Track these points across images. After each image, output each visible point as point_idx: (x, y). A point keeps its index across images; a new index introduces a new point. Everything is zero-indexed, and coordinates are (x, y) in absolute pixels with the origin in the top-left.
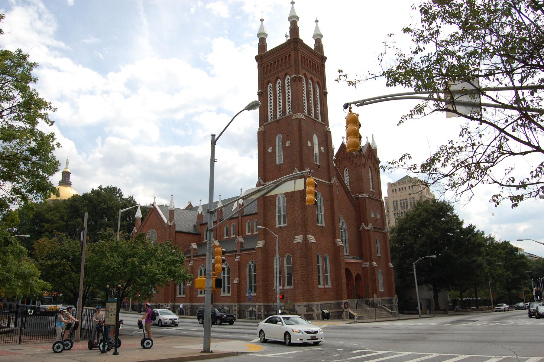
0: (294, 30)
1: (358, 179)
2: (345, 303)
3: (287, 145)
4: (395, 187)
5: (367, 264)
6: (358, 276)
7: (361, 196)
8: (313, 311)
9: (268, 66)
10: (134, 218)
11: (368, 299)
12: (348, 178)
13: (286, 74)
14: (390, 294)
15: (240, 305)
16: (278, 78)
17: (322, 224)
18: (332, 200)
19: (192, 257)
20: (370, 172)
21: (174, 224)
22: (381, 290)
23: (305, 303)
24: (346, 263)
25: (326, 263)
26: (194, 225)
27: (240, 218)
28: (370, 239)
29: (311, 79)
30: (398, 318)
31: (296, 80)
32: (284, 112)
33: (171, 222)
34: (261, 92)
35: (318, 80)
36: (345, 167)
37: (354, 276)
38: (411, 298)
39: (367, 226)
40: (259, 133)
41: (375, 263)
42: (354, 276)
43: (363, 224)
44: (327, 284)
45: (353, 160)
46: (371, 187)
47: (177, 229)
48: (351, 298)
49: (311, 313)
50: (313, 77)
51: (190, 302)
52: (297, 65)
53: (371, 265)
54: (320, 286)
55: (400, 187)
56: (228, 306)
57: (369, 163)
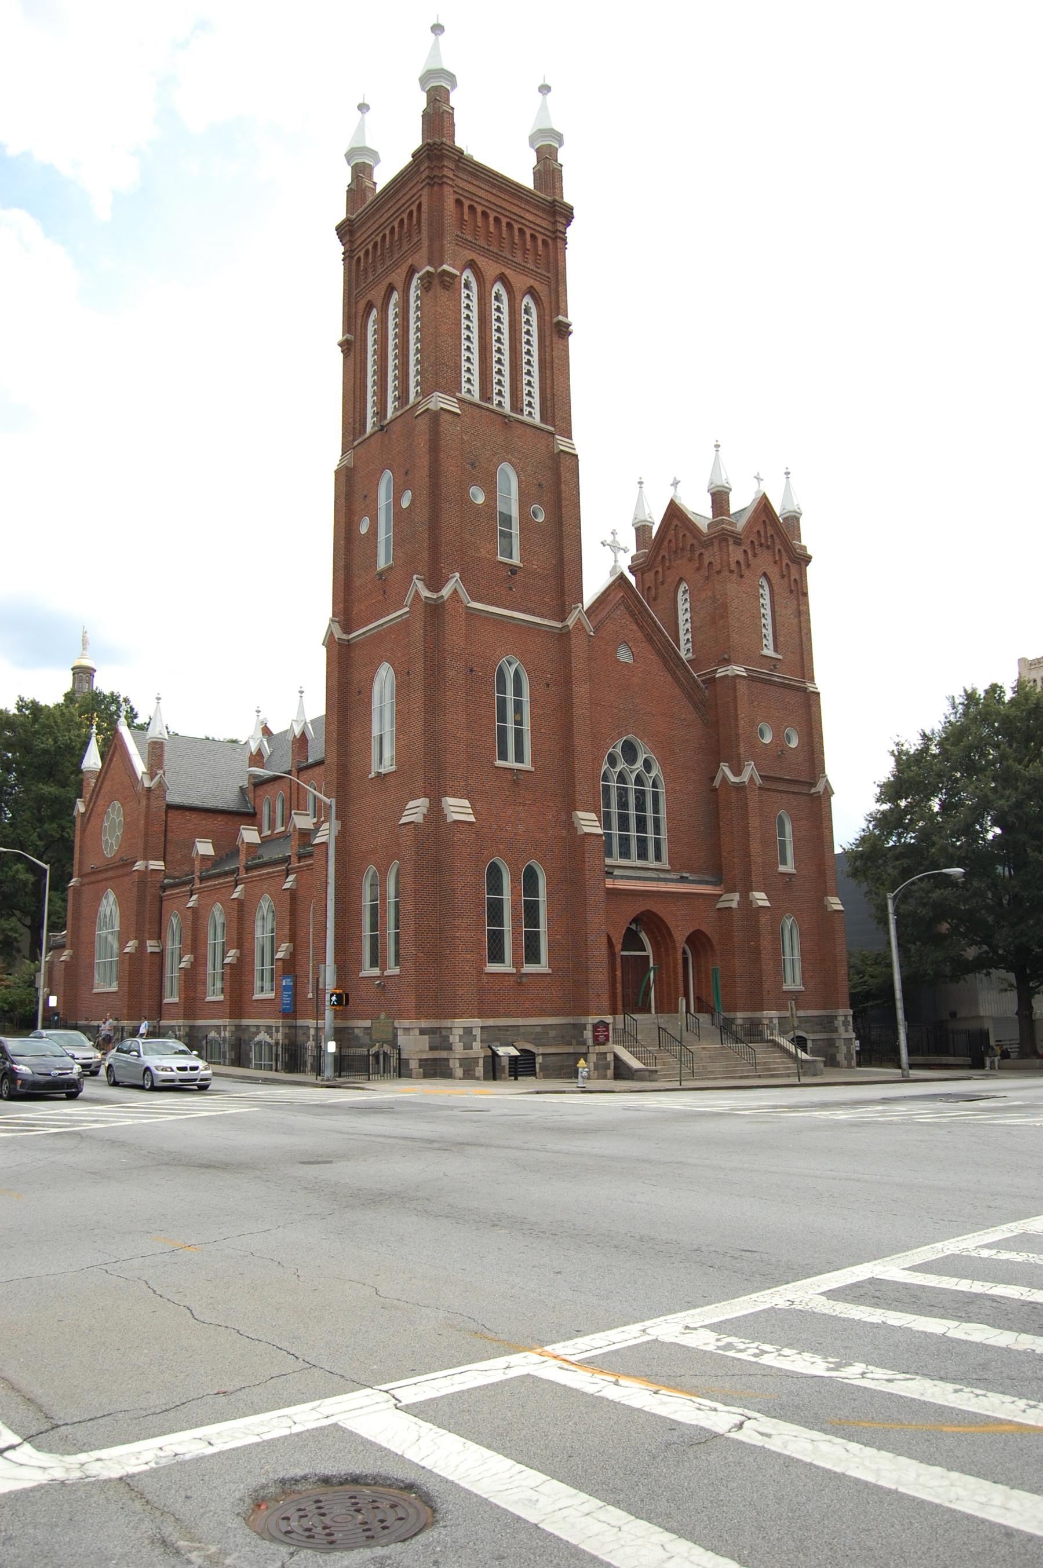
0: (438, 118)
2: (595, 1027)
5: (734, 900)
6: (697, 941)
8: (449, 1048)
10: (81, 771)
11: (731, 1015)
12: (688, 615)
13: (412, 271)
14: (828, 1001)
15: (238, 1027)
18: (566, 681)
19: (197, 881)
21: (161, 785)
22: (793, 981)
23: (424, 1024)
28: (745, 817)
29: (502, 278)
30: (676, 1085)
33: (152, 779)
35: (531, 282)
36: (681, 580)
37: (680, 936)
38: (953, 1015)
39: (737, 772)
42: (680, 936)
43: (725, 769)
45: (701, 554)
46: (769, 641)
47: (172, 798)
48: (669, 1012)
49: (444, 1054)
50: (508, 272)
51: (186, 1017)
52: (437, 234)
54: (492, 968)
57: (764, 561)
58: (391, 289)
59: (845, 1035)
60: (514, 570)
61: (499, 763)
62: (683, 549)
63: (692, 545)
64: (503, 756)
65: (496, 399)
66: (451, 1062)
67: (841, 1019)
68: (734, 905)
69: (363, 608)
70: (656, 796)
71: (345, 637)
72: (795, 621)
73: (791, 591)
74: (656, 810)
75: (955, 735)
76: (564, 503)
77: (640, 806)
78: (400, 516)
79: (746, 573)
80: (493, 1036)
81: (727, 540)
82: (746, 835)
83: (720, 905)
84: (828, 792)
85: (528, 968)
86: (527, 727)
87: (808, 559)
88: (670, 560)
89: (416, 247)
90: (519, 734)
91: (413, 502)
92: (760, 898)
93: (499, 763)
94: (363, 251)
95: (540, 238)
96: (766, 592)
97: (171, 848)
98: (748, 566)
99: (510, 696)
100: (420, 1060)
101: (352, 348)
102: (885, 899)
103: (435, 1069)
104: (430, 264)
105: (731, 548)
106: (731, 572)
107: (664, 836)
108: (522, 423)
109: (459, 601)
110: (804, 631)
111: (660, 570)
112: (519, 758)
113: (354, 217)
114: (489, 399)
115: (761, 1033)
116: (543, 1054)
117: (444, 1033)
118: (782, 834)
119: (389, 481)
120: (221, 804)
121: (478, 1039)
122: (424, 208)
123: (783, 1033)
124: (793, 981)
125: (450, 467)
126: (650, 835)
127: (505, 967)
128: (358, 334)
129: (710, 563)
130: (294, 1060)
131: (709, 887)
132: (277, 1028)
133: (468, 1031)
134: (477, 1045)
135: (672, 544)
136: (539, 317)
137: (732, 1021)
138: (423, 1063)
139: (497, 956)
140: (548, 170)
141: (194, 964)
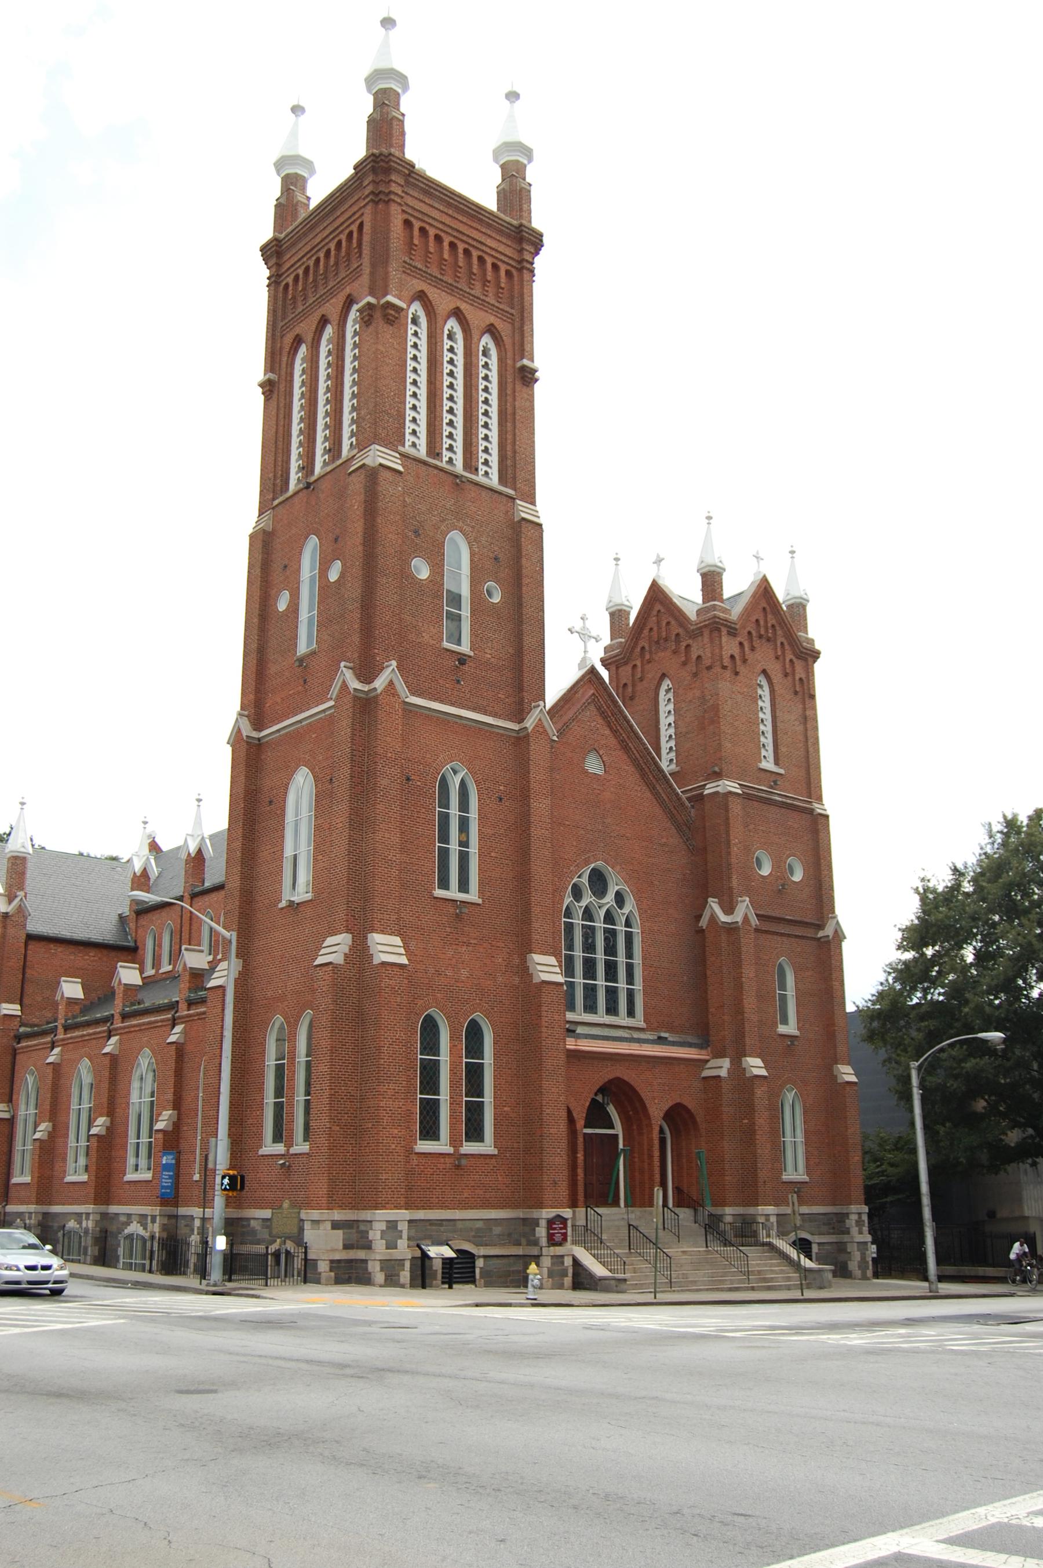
0: (385, 125)
2: (550, 1223)
5: (722, 1067)
6: (678, 1117)
8: (368, 1246)
11: (718, 1211)
12: (671, 719)
13: (350, 301)
14: (838, 1194)
15: (104, 1216)
18: (524, 795)
19: (60, 1030)
21: (21, 910)
22: (795, 1171)
23: (338, 1215)
24: (575, 1055)
26: (121, 917)
28: (738, 964)
30: (650, 1298)
32: (334, 450)
35: (492, 319)
36: (663, 676)
37: (657, 1110)
38: (992, 1215)
39: (729, 910)
41: (756, 1062)
42: (657, 1110)
43: (714, 905)
45: (688, 646)
46: (769, 752)
47: (34, 926)
48: (642, 1205)
49: (361, 1254)
50: (463, 306)
51: (39, 1201)
52: (381, 259)
54: (425, 1146)
57: (763, 656)
58: (324, 321)
59: (859, 1238)
60: (462, 659)
61: (439, 893)
62: (666, 640)
63: (678, 635)
64: (444, 884)
65: (446, 455)
66: (370, 1263)
67: (854, 1217)
68: (723, 1073)
69: (279, 700)
70: (629, 937)
71: (255, 734)
72: (801, 728)
73: (796, 693)
74: (629, 955)
75: (992, 870)
76: (525, 581)
77: (610, 949)
78: (326, 591)
79: (741, 668)
80: (424, 1233)
81: (719, 630)
82: (739, 987)
83: (706, 1073)
84: (839, 936)
85: (469, 1148)
86: (473, 850)
87: (815, 655)
88: (650, 652)
89: (357, 273)
90: (464, 858)
91: (342, 575)
92: (755, 1065)
93: (439, 893)
94: (292, 277)
95: (503, 268)
96: (765, 692)
97: (29, 989)
98: (745, 661)
99: (454, 811)
100: (332, 1261)
101: (275, 390)
102: (908, 1068)
103: (350, 1273)
104: (372, 293)
105: (724, 639)
106: (724, 668)
107: (638, 986)
108: (477, 484)
109: (395, 694)
110: (811, 741)
111: (639, 663)
112: (464, 887)
113: (282, 236)
114: (438, 455)
115: (755, 1234)
116: (485, 1257)
117: (362, 1227)
118: (783, 986)
119: (315, 549)
120: (95, 936)
121: (405, 1235)
122: (367, 228)
123: (782, 1234)
124: (795, 1171)
125: (389, 534)
126: (622, 985)
127: (442, 1146)
128: (283, 373)
129: (699, 657)
130: (172, 1258)
131: (693, 1050)
132: (154, 1218)
133: (392, 1225)
134: (403, 1243)
135: (653, 632)
136: (501, 361)
137: (719, 1218)
138: (335, 1264)
139: (430, 1131)
140: (515, 190)
141: (52, 1135)
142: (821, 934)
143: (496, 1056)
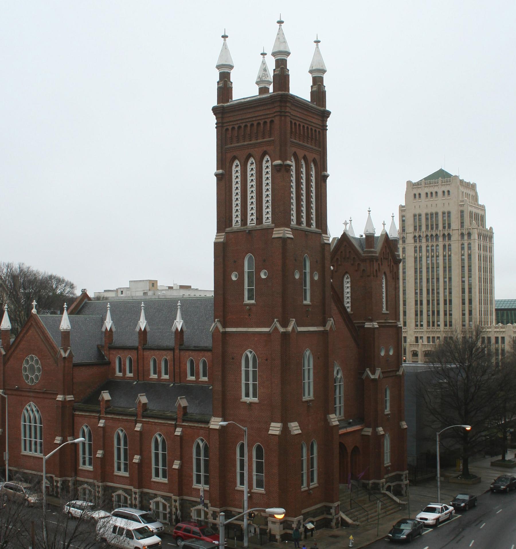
0: (282, 77)
1: (365, 296)
3: (263, 276)
4: (419, 191)
5: (368, 431)
6: (355, 450)
7: (368, 325)
9: (233, 128)
11: (366, 482)
16: (249, 156)
17: (308, 396)
20: (384, 281)
25: (312, 454)
27: (177, 351)
29: (305, 158)
31: (281, 171)
34: (222, 174)
35: (315, 156)
37: (349, 451)
39: (373, 373)
40: (216, 244)
42: (349, 451)
44: (312, 480)
45: (359, 264)
53: (375, 432)
55: (428, 190)
56: (163, 497)
57: (385, 268)
63: (354, 258)
67: (404, 476)
68: (370, 434)
73: (393, 278)
81: (373, 261)
92: (380, 430)
102: (436, 435)
115: (379, 490)
117: (289, 523)
129: (364, 270)
137: (368, 484)
142: (398, 373)
143: (318, 452)
